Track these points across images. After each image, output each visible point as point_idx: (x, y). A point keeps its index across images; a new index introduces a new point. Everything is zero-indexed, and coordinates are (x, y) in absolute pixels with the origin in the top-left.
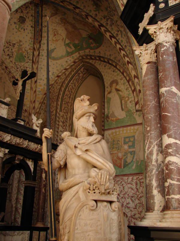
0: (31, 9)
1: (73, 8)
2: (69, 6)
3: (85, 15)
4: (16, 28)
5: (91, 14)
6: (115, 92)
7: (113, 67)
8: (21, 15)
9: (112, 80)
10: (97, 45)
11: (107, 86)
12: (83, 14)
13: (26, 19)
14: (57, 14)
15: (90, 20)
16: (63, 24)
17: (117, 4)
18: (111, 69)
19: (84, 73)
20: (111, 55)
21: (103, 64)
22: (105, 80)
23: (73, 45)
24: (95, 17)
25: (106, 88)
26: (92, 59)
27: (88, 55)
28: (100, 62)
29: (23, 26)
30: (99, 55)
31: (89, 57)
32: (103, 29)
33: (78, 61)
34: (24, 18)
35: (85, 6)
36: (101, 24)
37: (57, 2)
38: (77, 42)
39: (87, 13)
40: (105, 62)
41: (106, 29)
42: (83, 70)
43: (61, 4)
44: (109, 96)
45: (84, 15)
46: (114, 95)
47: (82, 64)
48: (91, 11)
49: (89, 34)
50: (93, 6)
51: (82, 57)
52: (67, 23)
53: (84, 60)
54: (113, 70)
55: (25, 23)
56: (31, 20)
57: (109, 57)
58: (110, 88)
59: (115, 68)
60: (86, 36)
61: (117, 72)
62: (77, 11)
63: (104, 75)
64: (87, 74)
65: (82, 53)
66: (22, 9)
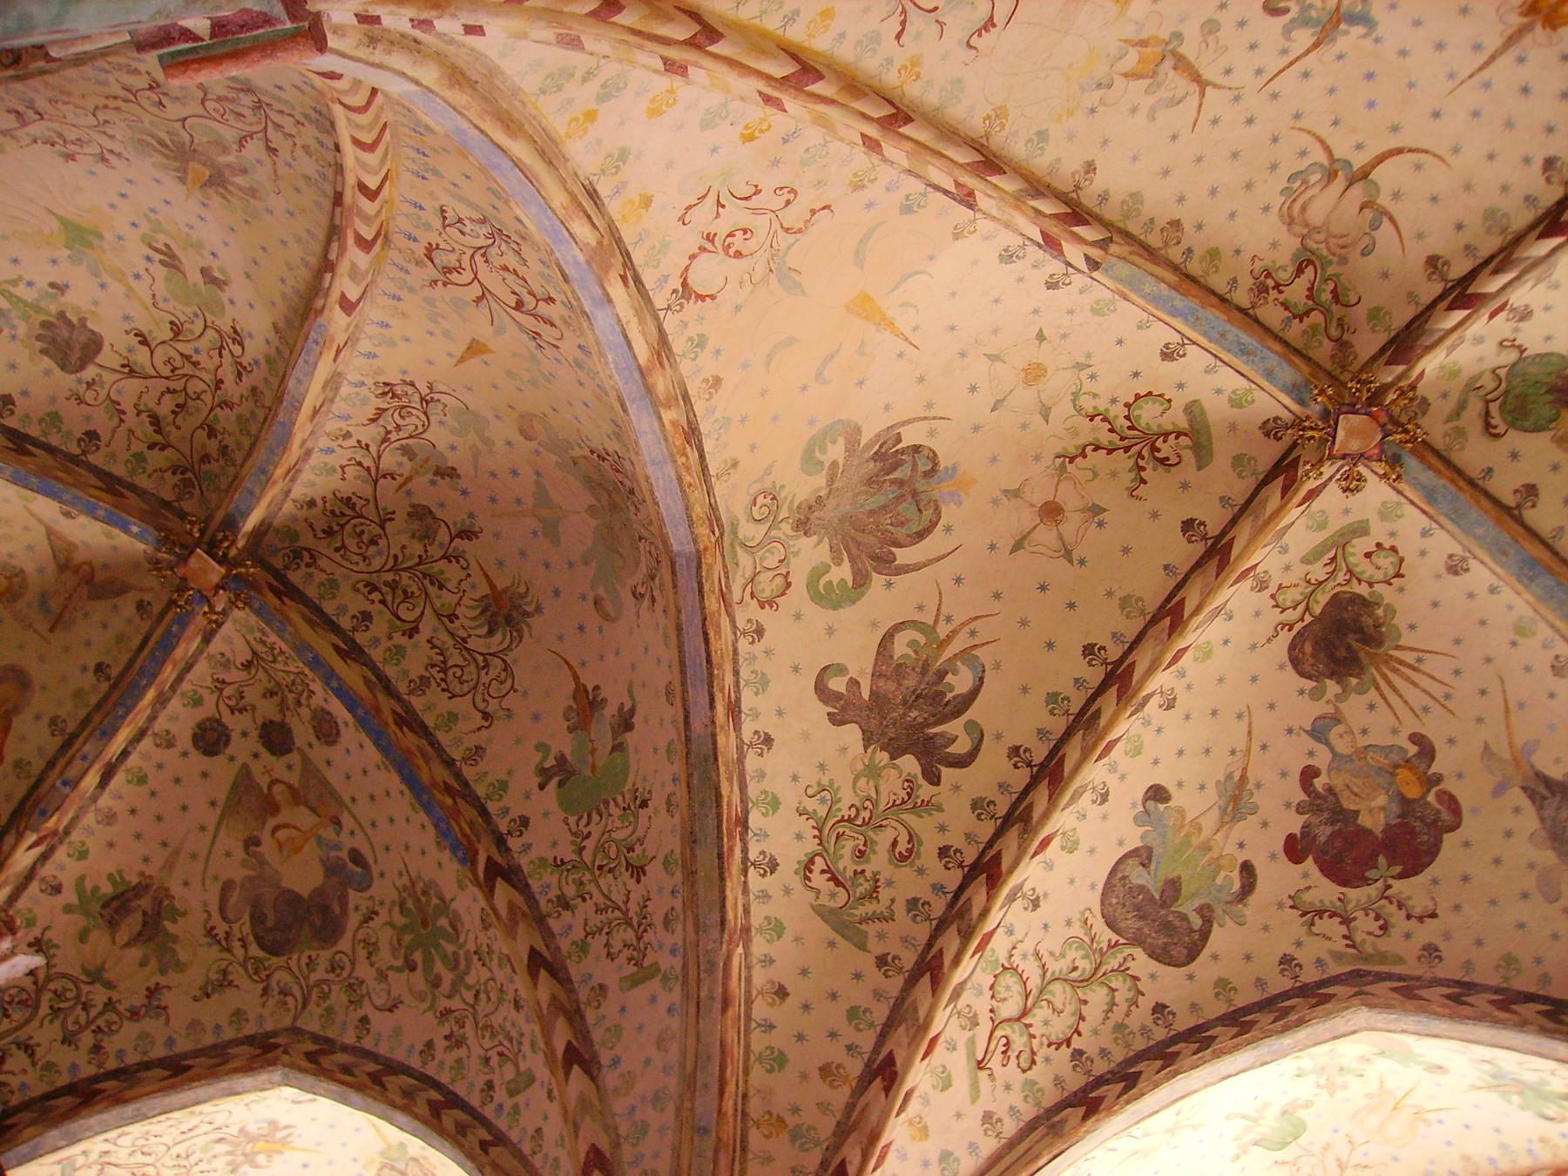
0: (139, 457)
4: (20, 279)
5: (61, 854)
8: (106, 349)
13: (71, 372)
17: (154, 1109)
24: (43, 880)
29: (22, 331)
34: (82, 367)
35: (110, 818)
39: (67, 832)
48: (83, 855)
50: (110, 877)
55: (43, 352)
56: (54, 418)
62: (91, 780)
66: (149, 382)
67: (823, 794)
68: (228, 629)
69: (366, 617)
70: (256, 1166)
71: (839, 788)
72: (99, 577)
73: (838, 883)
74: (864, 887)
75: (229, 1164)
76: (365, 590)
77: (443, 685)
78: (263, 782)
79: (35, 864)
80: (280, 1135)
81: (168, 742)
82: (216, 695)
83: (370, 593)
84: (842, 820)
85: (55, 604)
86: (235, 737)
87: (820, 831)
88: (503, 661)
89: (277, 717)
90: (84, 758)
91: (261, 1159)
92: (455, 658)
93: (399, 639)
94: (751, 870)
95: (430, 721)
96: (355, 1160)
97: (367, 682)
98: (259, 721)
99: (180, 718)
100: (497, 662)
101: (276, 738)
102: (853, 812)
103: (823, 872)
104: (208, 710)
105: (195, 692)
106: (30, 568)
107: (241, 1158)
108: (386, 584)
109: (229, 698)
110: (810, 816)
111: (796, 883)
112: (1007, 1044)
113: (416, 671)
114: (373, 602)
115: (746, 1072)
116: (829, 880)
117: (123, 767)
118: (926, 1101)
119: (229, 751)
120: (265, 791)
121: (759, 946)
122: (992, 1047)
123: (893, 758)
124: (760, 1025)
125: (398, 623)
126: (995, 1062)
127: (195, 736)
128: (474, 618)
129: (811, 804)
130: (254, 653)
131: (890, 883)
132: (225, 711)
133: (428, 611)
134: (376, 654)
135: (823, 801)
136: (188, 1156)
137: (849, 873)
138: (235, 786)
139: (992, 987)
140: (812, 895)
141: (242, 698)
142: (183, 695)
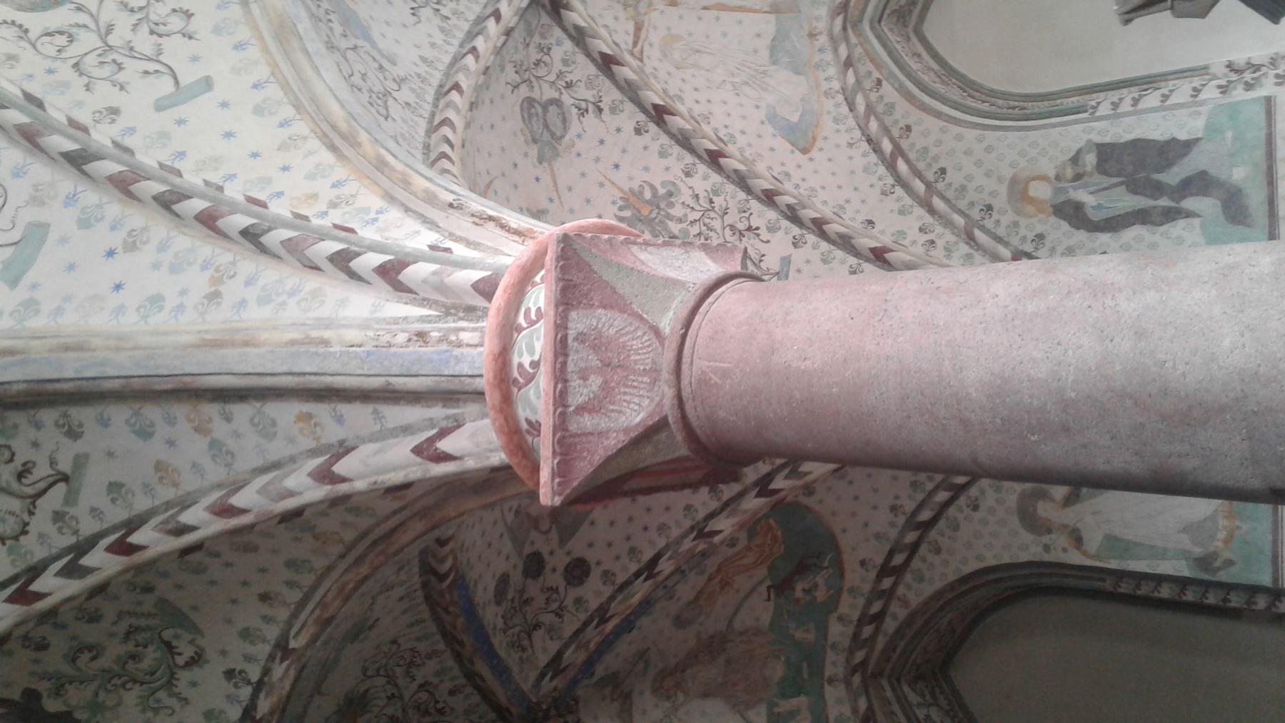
1: (649, 582)
2: (633, 596)
3: (694, 540)
5: (701, 514)
6: (1078, 507)
7: (952, 511)
9: (1014, 522)
10: (826, 564)
11: (1040, 549)
12: (687, 544)
14: (631, 692)
15: (725, 525)
16: (681, 697)
18: (960, 517)
19: (928, 697)
20: (899, 503)
21: (924, 560)
22: (1006, 560)
23: (784, 696)
24: (719, 499)
25: (1047, 558)
26: (878, 618)
27: (856, 636)
28: (908, 577)
30: (873, 574)
31: (867, 631)
32: (779, 483)
33: (869, 700)
36: (756, 484)
37: (597, 640)
38: (777, 670)
39: (692, 528)
40: (914, 548)
41: (786, 471)
42: (914, 691)
43: (610, 626)
44: (1093, 541)
45: (696, 546)
46: (1095, 513)
47: (888, 688)
48: (688, 508)
49: (768, 583)
51: (854, 671)
52: (683, 671)
53: (871, 668)
54: (967, 511)
57: (901, 520)
58: (1053, 536)
59: (962, 500)
60: (772, 604)
61: (982, 492)
62: (665, 566)
63: (980, 558)
64: (937, 690)
65: (834, 664)
67: (156, 706)
68: (543, 660)
69: (452, 693)
70: (653, 188)
71: (137, 705)
72: (608, 690)
73: (169, 646)
74: (140, 637)
75: (671, 205)
76: (447, 709)
77: (416, 654)
78: (554, 535)
79: (720, 513)
80: (627, 213)
81: (607, 576)
82: (565, 603)
83: (444, 707)
84: (142, 684)
85: (641, 666)
86: (561, 568)
87: (169, 682)
88: (365, 675)
89: (530, 581)
90: (665, 587)
91: (648, 195)
92: (399, 671)
93: (435, 681)
94: (254, 678)
95: (438, 637)
96: (579, 155)
97: (472, 663)
98: (541, 578)
99: (594, 591)
100: (369, 673)
101: (535, 565)
102: (128, 686)
103: (180, 654)
104: (573, 593)
105: (577, 609)
106: (648, 693)
107: (663, 205)
108: (430, 714)
109: (556, 600)
110: (177, 695)
111: (211, 654)
112: (20, 476)
113: (432, 666)
114: (444, 702)
115: (329, 569)
116: (176, 647)
117: (642, 564)
118: (148, 489)
119: (567, 560)
120: (554, 526)
121: (272, 633)
122: (42, 485)
123: (69, 713)
124: (300, 588)
125: (431, 690)
126: (42, 470)
127: (587, 576)
128: (375, 698)
129: (173, 702)
130: (530, 636)
131: (112, 635)
132: (562, 590)
133: (407, 698)
134: (456, 671)
135: (158, 701)
136: (699, 234)
137: (150, 649)
138: (572, 534)
139: (24, 532)
140: (201, 642)
141: (547, 599)
142: (586, 611)
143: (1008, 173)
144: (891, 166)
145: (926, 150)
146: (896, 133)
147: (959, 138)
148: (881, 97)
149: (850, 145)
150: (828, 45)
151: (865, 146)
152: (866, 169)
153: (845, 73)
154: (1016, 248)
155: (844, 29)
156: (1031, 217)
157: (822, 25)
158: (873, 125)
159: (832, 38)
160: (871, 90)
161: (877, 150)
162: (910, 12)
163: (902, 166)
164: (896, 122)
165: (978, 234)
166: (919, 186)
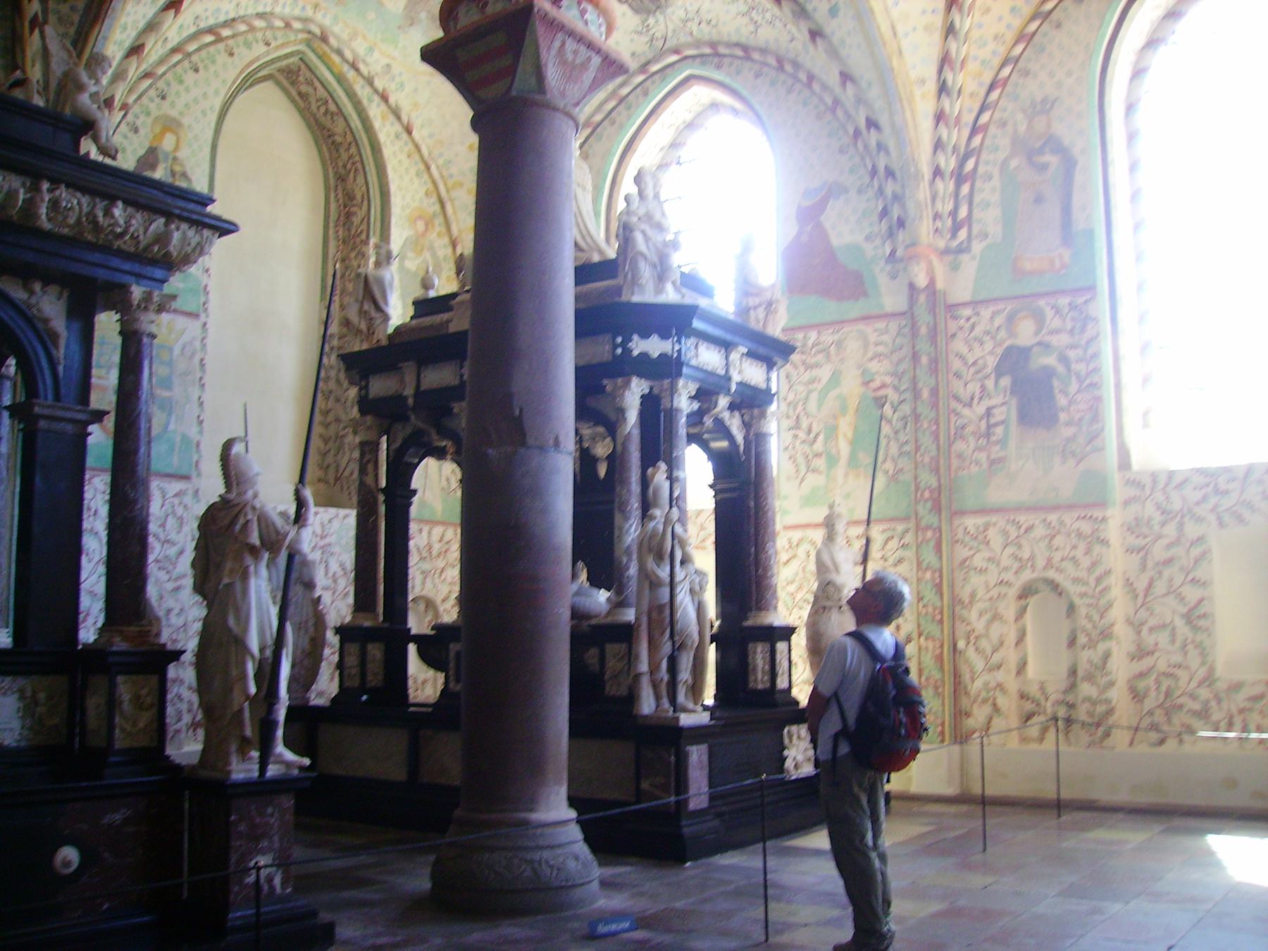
143: (186, 121)
144: (210, 30)
145: (214, 62)
146: (231, 42)
147: (217, 93)
148: (257, 41)
149: (238, 5)
150: (304, 15)
151: (231, 16)
152: (218, 10)
153: (282, 19)
154: (132, 107)
155: (309, 32)
156: (152, 128)
157: (319, 17)
158: (243, 28)
159: (305, 20)
160: (264, 35)
161: (226, 24)
162: (287, 79)
163: (209, 38)
164: (238, 46)
165: (147, 83)
166: (191, 47)
